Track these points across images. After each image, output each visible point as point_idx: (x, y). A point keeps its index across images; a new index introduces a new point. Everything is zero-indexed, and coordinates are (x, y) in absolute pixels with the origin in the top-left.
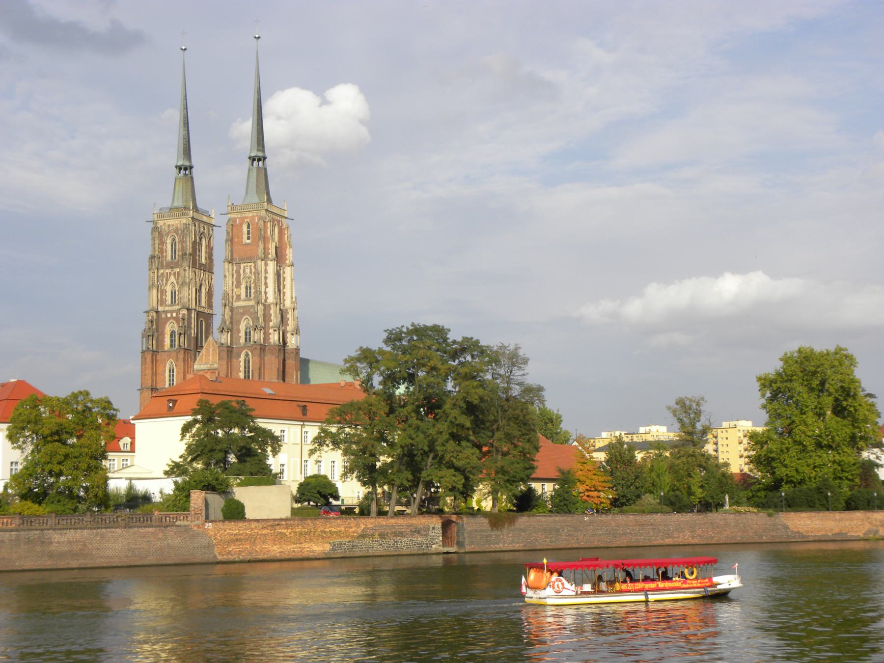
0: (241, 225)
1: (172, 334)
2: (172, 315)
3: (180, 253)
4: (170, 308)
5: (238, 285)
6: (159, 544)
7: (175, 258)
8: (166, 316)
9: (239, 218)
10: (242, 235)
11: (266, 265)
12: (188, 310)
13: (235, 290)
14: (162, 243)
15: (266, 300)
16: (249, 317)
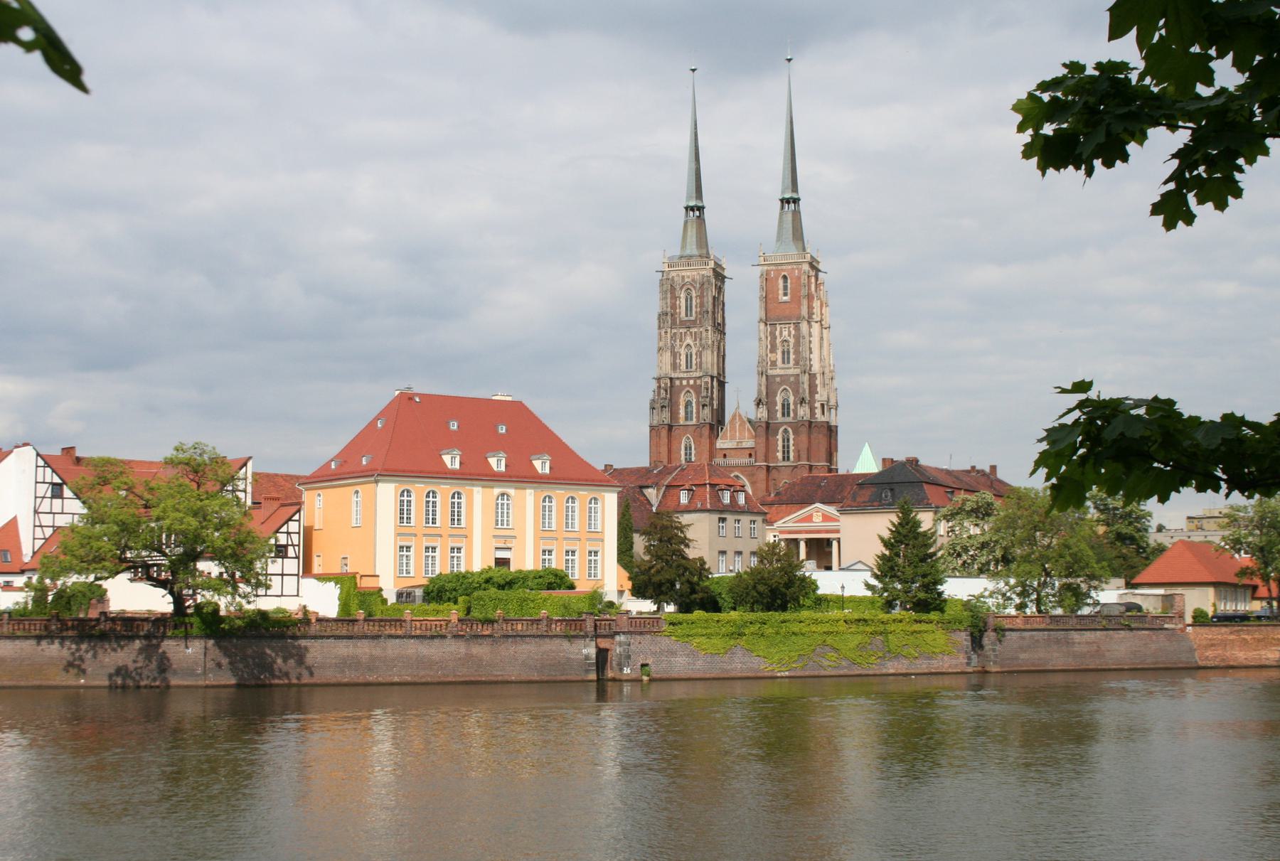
0: (777, 279)
1: (688, 404)
2: (688, 382)
3: (698, 310)
4: (685, 375)
5: (773, 350)
6: (1153, 646)
7: (691, 316)
8: (681, 383)
9: (774, 270)
10: (778, 290)
11: (810, 327)
12: (712, 378)
13: (769, 355)
14: (675, 298)
15: (810, 370)
16: (788, 388)
